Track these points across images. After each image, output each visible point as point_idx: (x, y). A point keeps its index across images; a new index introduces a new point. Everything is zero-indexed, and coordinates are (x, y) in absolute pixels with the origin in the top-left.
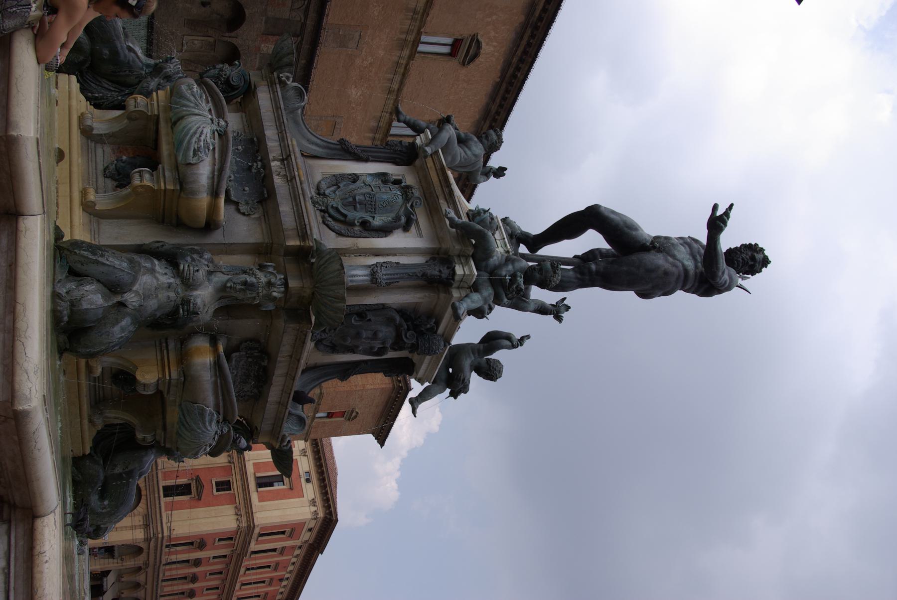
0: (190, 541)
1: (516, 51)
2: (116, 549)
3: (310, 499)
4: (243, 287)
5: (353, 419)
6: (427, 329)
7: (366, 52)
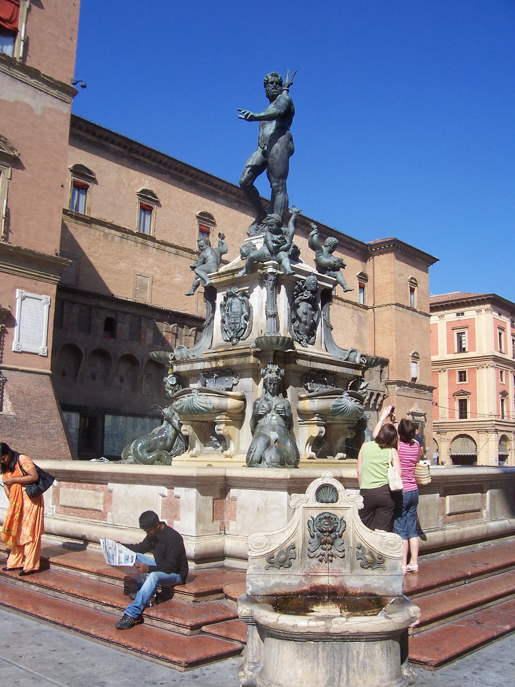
0: (501, 401)
1: (148, 163)
2: (500, 453)
3: (476, 314)
4: (272, 385)
5: (416, 281)
6: (303, 285)
7: (150, 271)
